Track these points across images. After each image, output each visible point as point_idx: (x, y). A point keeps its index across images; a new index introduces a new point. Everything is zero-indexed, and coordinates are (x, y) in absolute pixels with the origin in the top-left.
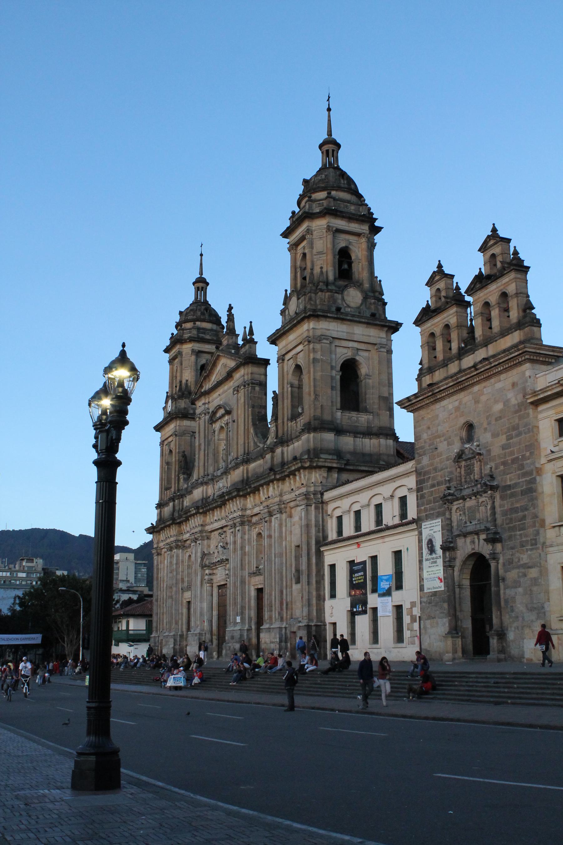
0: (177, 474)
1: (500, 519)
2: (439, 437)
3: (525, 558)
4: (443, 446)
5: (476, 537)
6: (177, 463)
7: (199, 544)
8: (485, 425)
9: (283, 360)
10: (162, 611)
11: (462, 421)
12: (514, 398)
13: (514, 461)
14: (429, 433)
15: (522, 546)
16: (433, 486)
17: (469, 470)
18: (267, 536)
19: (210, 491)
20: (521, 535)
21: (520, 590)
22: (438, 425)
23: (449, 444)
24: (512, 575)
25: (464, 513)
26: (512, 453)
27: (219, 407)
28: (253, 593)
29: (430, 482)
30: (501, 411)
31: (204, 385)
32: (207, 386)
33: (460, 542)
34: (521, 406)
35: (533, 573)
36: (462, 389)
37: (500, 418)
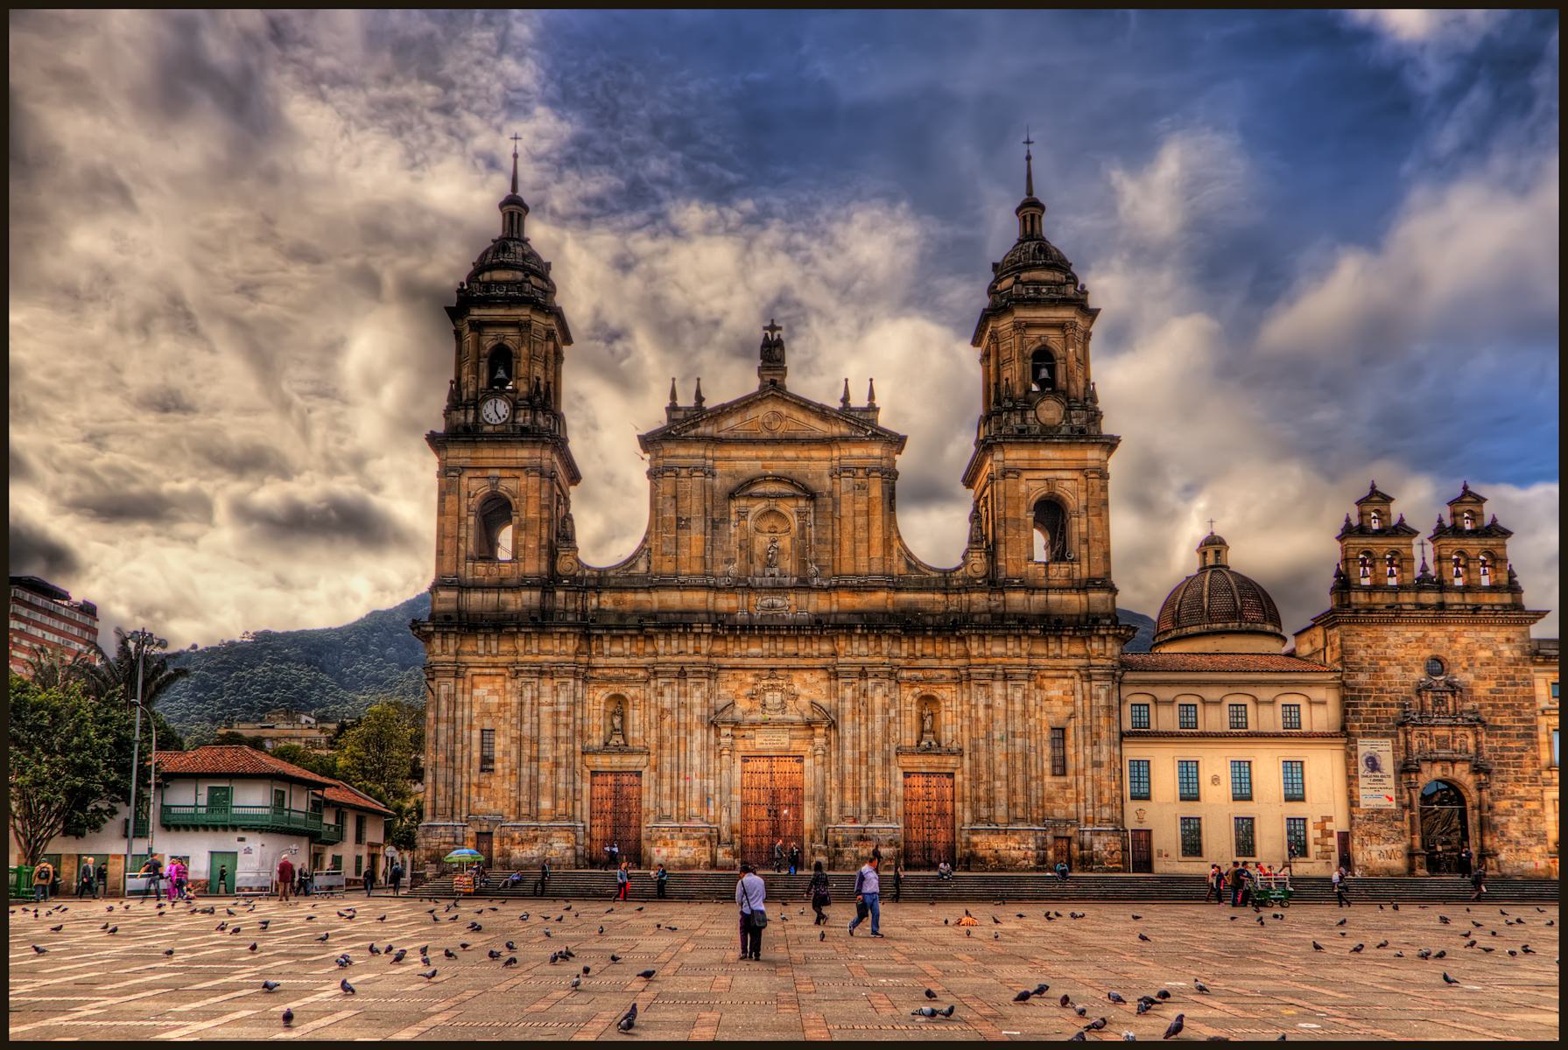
0: (544, 542)
1: (1486, 754)
2: (1389, 660)
3: (1521, 792)
4: (1395, 671)
5: (1449, 764)
6: (545, 525)
7: (698, 683)
8: (1465, 665)
9: (1019, 474)
10: (465, 780)
11: (1427, 653)
12: (1507, 652)
13: (1506, 706)
14: (1370, 651)
15: (1517, 780)
16: (1374, 705)
17: (1439, 702)
18: (988, 707)
19: (725, 603)
20: (1516, 772)
21: (1515, 818)
22: (1388, 647)
23: (1404, 670)
24: (1504, 804)
25: (1431, 741)
26: (1503, 699)
27: (778, 479)
28: (900, 777)
29: (1369, 702)
30: (1488, 658)
31: (702, 424)
32: (706, 429)
33: (1425, 767)
34: (1516, 662)
35: (1534, 805)
36: (1432, 624)
37: (1488, 664)
